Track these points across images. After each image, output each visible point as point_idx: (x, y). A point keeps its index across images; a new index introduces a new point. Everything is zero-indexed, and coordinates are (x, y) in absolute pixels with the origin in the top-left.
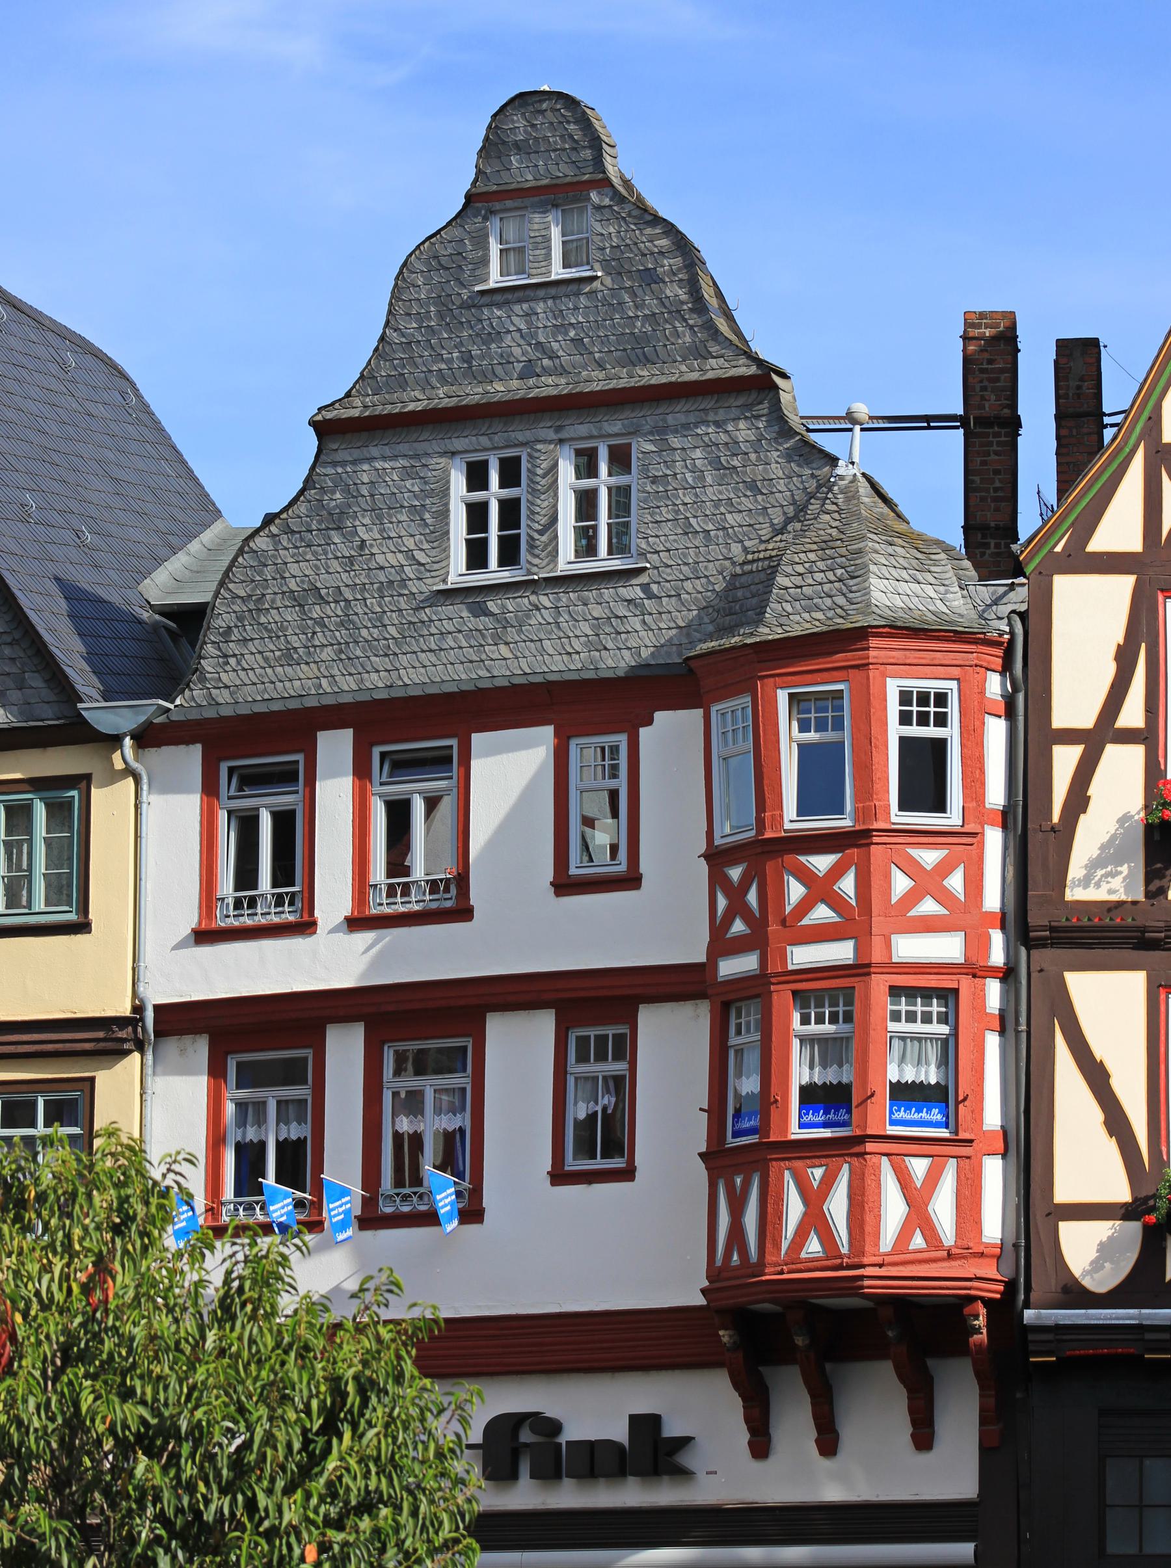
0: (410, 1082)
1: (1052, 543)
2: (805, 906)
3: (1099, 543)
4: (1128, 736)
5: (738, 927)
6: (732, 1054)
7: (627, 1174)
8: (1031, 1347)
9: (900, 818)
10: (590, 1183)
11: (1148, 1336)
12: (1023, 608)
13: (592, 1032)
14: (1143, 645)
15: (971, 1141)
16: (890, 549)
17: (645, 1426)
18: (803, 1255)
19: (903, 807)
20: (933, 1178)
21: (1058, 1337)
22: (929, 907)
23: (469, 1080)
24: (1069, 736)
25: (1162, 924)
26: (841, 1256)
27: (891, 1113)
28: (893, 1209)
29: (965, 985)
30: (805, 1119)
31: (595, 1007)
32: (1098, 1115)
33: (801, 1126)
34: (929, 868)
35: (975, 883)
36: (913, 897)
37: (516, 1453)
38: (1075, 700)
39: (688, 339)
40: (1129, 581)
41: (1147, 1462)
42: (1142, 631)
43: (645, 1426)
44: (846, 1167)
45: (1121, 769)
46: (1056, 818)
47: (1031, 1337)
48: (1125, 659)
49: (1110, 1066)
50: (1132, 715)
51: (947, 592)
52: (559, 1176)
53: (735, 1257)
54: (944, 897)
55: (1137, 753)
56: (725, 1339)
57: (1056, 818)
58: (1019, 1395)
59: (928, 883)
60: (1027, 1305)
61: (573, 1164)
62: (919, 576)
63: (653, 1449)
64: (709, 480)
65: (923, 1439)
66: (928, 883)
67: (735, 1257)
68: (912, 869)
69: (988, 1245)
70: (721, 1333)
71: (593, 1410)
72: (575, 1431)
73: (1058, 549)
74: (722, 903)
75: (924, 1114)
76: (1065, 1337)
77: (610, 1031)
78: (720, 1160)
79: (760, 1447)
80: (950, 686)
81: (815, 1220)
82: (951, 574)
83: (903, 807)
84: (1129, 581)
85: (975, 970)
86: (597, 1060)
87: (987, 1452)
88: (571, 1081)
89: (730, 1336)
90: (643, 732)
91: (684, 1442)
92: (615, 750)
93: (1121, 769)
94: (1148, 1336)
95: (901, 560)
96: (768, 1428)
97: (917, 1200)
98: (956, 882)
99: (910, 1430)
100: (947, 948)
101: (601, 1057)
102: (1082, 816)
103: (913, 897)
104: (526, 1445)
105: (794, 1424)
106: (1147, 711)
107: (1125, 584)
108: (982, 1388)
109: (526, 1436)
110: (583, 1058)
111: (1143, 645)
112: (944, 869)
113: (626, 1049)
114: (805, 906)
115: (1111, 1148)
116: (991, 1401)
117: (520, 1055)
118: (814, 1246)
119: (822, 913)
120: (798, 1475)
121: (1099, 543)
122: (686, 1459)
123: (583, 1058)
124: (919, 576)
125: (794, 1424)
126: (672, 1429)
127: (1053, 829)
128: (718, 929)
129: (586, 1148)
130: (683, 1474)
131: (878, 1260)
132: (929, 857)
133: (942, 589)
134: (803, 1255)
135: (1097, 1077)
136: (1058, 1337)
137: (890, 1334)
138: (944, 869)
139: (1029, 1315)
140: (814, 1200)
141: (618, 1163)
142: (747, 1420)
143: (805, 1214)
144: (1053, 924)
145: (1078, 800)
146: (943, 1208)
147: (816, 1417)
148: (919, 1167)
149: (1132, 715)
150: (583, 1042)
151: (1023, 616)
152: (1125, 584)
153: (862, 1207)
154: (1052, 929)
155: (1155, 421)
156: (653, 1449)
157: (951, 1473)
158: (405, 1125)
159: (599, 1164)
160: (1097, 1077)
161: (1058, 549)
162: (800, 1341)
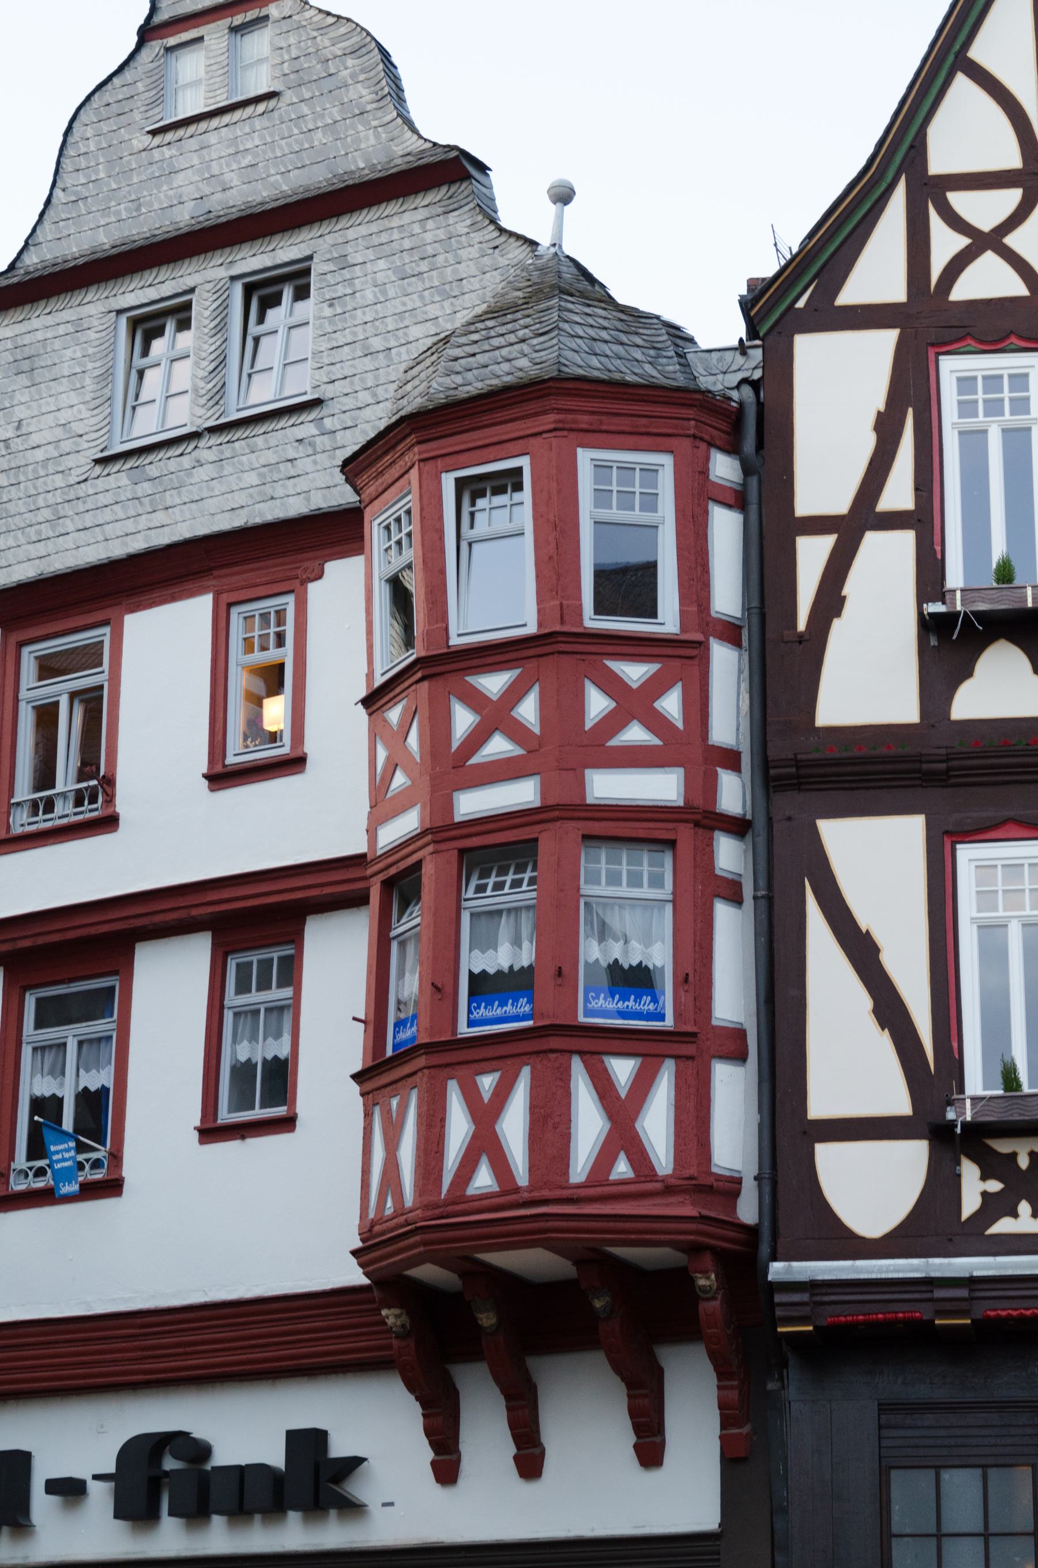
0: (51, 1034)
1: (794, 294)
2: (477, 738)
3: (850, 295)
4: (893, 521)
5: (400, 780)
6: (394, 946)
7: (287, 1124)
8: (779, 1312)
9: (592, 621)
10: (243, 1138)
11: (939, 1293)
12: (758, 374)
13: (254, 958)
14: (910, 411)
15: (694, 1035)
16: (588, 310)
17: (308, 1444)
18: (471, 1191)
19: (600, 608)
20: (643, 1084)
21: (818, 1298)
22: (635, 734)
23: (114, 1026)
24: (817, 525)
25: (943, 751)
26: (517, 1190)
27: (586, 1000)
28: (589, 1124)
29: (685, 834)
30: (476, 1015)
31: (254, 921)
32: (865, 1002)
33: (471, 1024)
34: (635, 686)
35: (698, 706)
36: (613, 722)
37: (156, 1482)
38: (825, 472)
39: (372, 141)
40: (889, 338)
41: (946, 1475)
42: (911, 394)
43: (308, 1444)
44: (526, 1073)
45: (886, 562)
46: (802, 625)
47: (778, 1298)
48: (887, 429)
49: (880, 937)
50: (898, 493)
51: (658, 357)
52: (211, 1132)
53: (389, 1203)
54: (656, 722)
55: (905, 540)
56: (391, 1321)
57: (802, 625)
58: (771, 1386)
59: (635, 704)
60: (775, 1259)
61: (225, 1116)
62: (624, 338)
63: (316, 1476)
64: (391, 293)
65: (650, 1452)
66: (635, 704)
67: (389, 1203)
68: (612, 685)
69: (719, 1178)
70: (384, 1312)
71: (244, 1428)
72: (228, 1453)
73: (801, 304)
74: (382, 754)
75: (631, 1003)
76: (826, 1299)
77: (275, 954)
78: (375, 1076)
79: (446, 1471)
80: (665, 462)
81: (485, 1143)
82: (665, 337)
83: (600, 608)
84: (889, 338)
85: (700, 817)
86: (258, 990)
87: (734, 1463)
88: (228, 1017)
89: (397, 1316)
90: (312, 587)
91: (354, 1463)
92: (280, 615)
93: (886, 562)
94: (939, 1293)
95: (600, 321)
96: (457, 1442)
97: (622, 1113)
98: (671, 704)
99: (632, 1439)
100: (663, 787)
101: (264, 985)
102: (836, 623)
103: (613, 722)
104: (167, 1474)
105: (486, 1436)
106: (917, 489)
107: (884, 342)
108: (722, 1374)
109: (170, 1464)
110: (243, 987)
111: (910, 411)
112: (656, 687)
113: (291, 972)
114: (477, 738)
115: (883, 1044)
116: (734, 1395)
117: (170, 987)
118: (484, 1180)
119: (498, 746)
120: (491, 1505)
121: (850, 295)
122: (358, 1488)
123: (243, 987)
124: (624, 338)
125: (486, 1436)
126: (339, 1448)
127: (801, 638)
128: (378, 789)
129: (243, 1100)
130: (352, 1508)
131: (565, 1193)
132: (635, 672)
133: (652, 352)
134: (471, 1191)
135: (862, 951)
136: (818, 1298)
137: (598, 1304)
138: (656, 687)
139: (778, 1270)
140: (486, 1115)
141: (280, 1111)
142: (429, 1432)
143: (474, 1137)
144: (799, 757)
145: (830, 600)
146: (657, 1125)
147: (513, 1425)
148: (623, 1070)
149: (898, 493)
150: (244, 970)
151: (755, 385)
152: (884, 342)
153: (550, 1124)
154: (798, 763)
155: (919, 149)
156: (316, 1476)
157: (686, 1495)
158: (43, 1086)
159: (258, 1113)
160: (862, 951)
161: (801, 304)
162: (487, 1320)
